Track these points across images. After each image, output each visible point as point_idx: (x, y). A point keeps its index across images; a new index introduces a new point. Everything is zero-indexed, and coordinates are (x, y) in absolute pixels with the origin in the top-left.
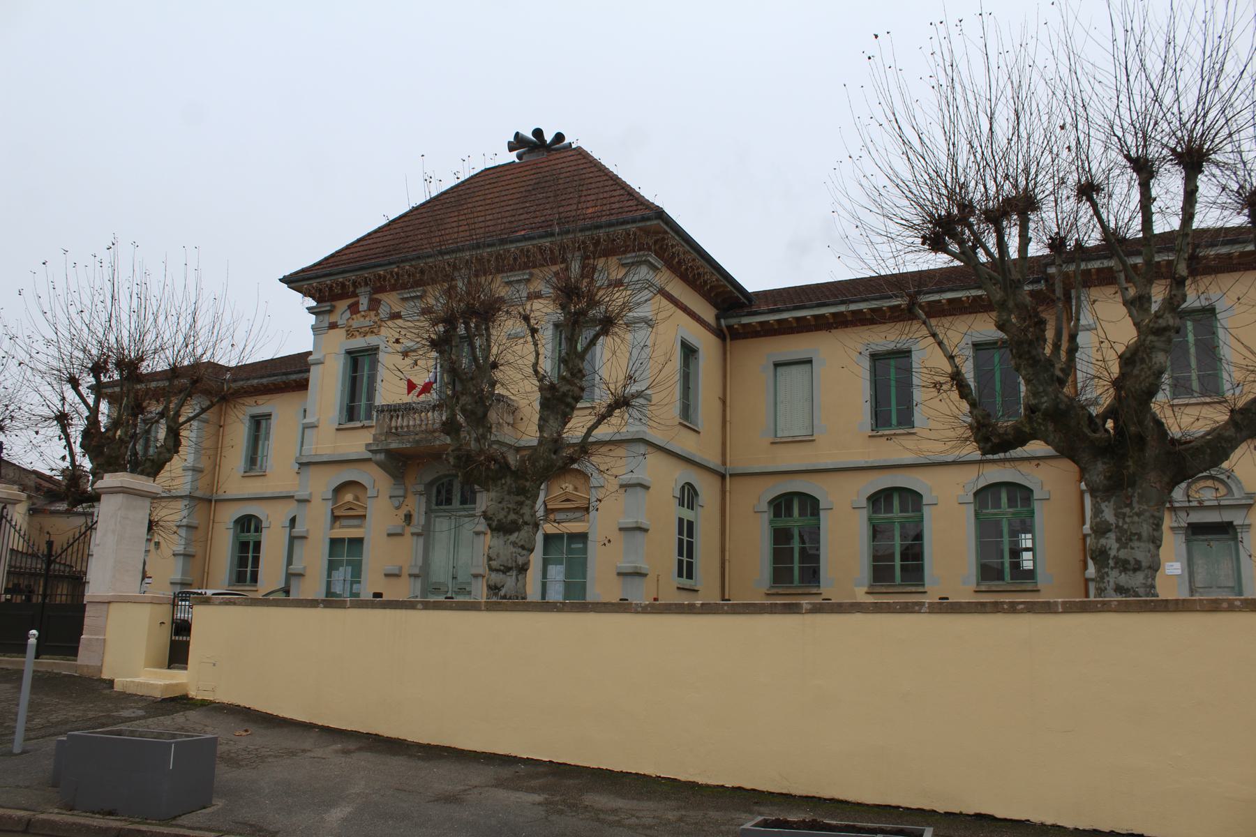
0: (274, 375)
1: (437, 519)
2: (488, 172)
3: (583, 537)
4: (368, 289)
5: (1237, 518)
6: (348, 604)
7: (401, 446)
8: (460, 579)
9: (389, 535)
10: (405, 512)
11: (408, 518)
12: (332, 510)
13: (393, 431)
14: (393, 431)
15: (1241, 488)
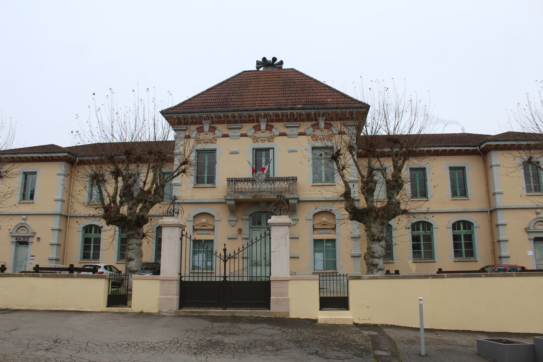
1: (253, 232)
3: (333, 241)
6: (446, 276)
7: (245, 198)
9: (229, 239)
10: (238, 228)
11: (240, 231)
12: (193, 226)
14: (236, 190)
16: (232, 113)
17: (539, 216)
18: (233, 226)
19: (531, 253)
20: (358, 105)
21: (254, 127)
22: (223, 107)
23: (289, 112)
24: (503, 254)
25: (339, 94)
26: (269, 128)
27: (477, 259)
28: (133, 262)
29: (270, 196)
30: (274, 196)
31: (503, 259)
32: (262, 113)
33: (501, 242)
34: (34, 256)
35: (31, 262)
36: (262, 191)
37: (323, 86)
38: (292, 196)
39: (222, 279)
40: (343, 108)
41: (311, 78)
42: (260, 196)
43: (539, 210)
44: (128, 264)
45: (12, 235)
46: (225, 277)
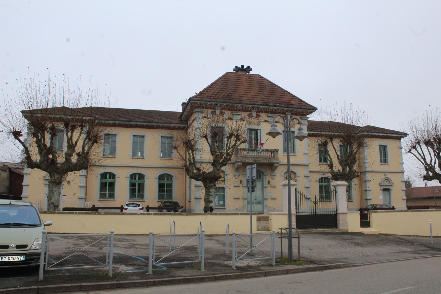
0: (121, 121)
4: (220, 108)
5: (390, 188)
7: (249, 161)
11: (241, 182)
15: (392, 182)
16: (237, 104)
17: (386, 176)
18: (237, 179)
19: (381, 197)
20: (310, 108)
21: (248, 115)
23: (272, 108)
24: (368, 198)
26: (258, 116)
27: (353, 200)
28: (212, 203)
30: (266, 161)
31: (368, 200)
32: (256, 106)
33: (368, 191)
35: (63, 200)
37: (284, 91)
38: (277, 162)
39: (314, 213)
40: (303, 109)
41: (274, 84)
43: (386, 173)
44: (209, 204)
45: (46, 179)
46: (316, 212)
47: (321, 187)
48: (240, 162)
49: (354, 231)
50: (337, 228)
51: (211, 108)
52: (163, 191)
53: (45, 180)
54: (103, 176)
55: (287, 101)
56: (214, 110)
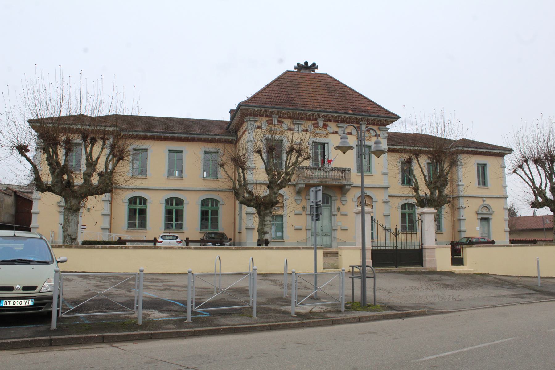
0: (153, 132)
2: (289, 73)
7: (314, 183)
8: (324, 231)
11: (304, 208)
13: (308, 176)
15: (492, 210)
17: (485, 203)
18: (298, 204)
19: (478, 228)
20: (391, 116)
21: (313, 124)
22: (290, 105)
23: (343, 115)
24: (462, 229)
25: (373, 104)
26: (325, 126)
27: (443, 232)
29: (333, 182)
30: (336, 182)
32: (323, 114)
34: (85, 226)
35: (82, 231)
36: (326, 178)
37: (358, 94)
38: (348, 183)
39: (395, 248)
40: (382, 117)
41: (346, 86)
42: (326, 182)
43: (485, 199)
44: (264, 236)
45: (60, 205)
46: (396, 246)
47: (403, 215)
48: (303, 184)
49: (443, 270)
50: (423, 266)
51: (267, 116)
52: (207, 220)
53: (59, 206)
54: (132, 201)
55: (362, 108)
56: (271, 118)
